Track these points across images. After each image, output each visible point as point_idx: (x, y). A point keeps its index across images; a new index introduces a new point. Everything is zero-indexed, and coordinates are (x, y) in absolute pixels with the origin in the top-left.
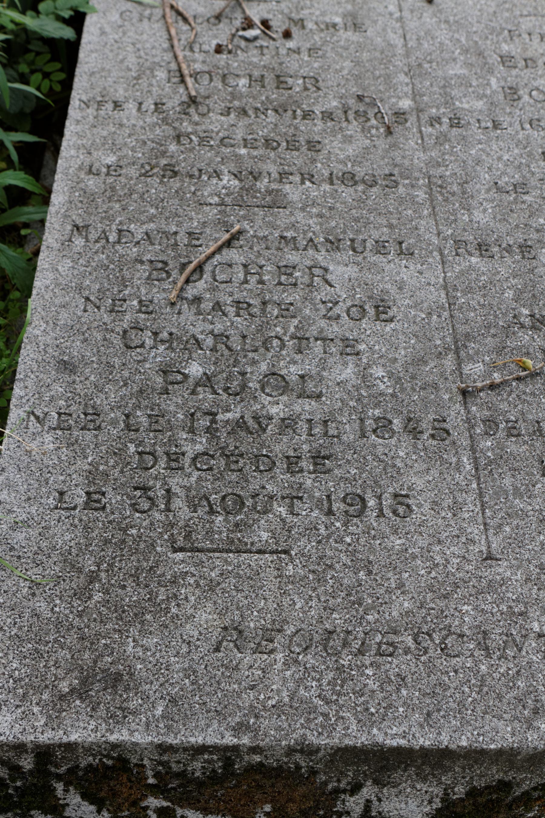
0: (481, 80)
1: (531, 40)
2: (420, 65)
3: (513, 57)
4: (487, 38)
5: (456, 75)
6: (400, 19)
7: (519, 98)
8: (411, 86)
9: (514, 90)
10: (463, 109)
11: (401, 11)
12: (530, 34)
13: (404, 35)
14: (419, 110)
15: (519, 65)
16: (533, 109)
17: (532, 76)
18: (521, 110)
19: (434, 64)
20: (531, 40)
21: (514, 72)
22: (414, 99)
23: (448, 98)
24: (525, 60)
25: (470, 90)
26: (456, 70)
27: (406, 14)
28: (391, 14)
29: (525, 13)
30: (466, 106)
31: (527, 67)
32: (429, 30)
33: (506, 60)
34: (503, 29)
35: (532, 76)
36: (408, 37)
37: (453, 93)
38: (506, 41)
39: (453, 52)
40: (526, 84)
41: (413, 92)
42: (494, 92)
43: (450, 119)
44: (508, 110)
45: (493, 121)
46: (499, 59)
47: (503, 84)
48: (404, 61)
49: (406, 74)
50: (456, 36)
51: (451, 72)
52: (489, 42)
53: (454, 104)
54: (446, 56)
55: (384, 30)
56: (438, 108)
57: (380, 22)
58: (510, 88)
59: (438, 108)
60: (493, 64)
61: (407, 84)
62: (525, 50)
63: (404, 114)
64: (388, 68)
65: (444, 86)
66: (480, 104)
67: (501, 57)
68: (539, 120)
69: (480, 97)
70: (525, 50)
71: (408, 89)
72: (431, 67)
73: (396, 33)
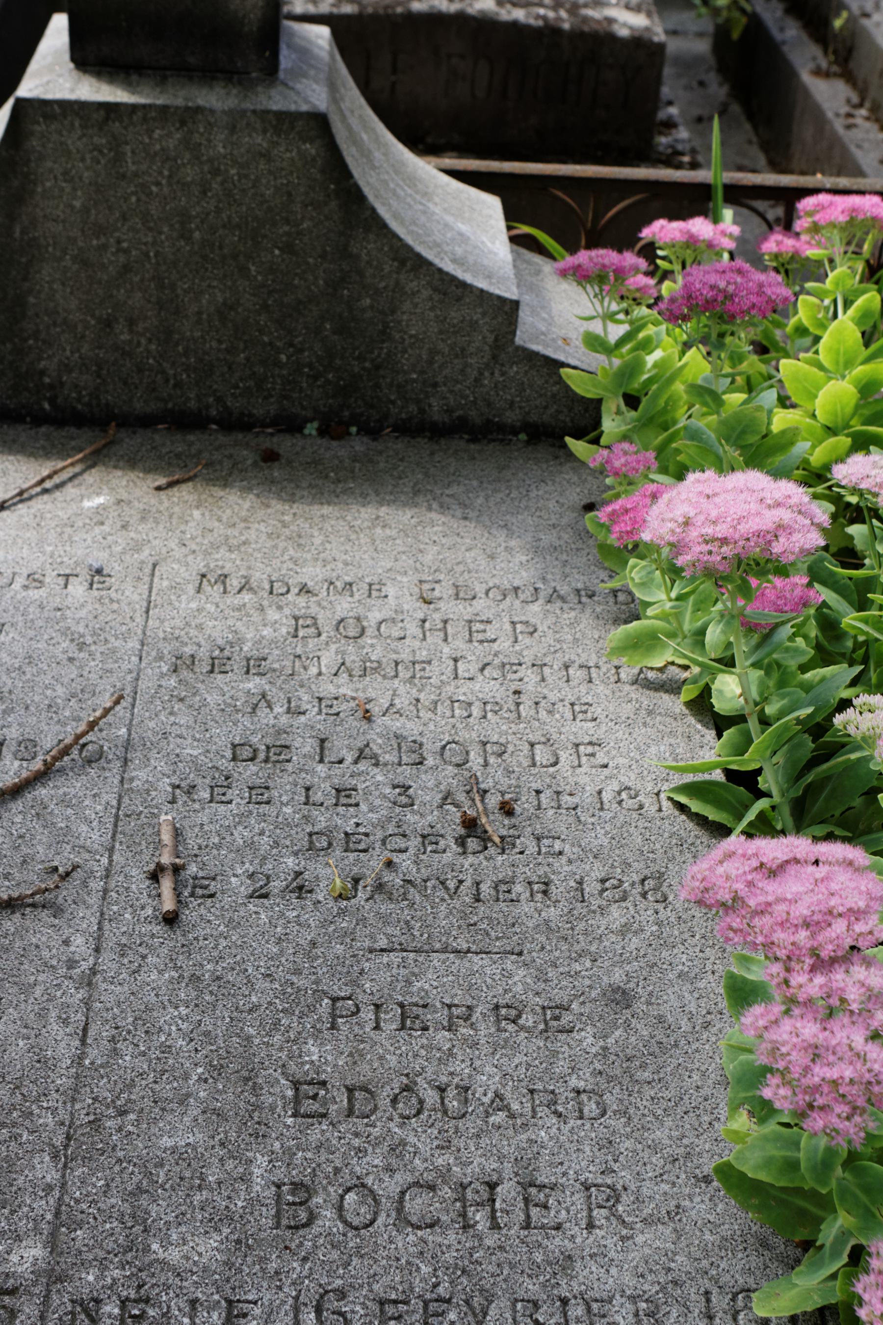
0: (230, 1164)
1: (377, 1027)
2: (96, 1124)
3: (323, 1083)
4: (277, 1024)
5: (174, 1150)
6: (88, 981)
7: (312, 1218)
8: (56, 1193)
9: (303, 1189)
10: (163, 1262)
11: (97, 950)
12: (377, 1007)
13: (85, 1030)
14: (53, 1277)
15: (333, 1108)
16: (335, 1255)
17: (356, 1142)
18: (305, 1259)
19: (132, 1116)
20: (377, 1027)
21: (317, 1132)
22: (52, 1244)
23: (138, 1229)
24: (350, 1090)
25: (197, 1198)
26: (179, 1134)
27: (108, 961)
28: (71, 964)
29: (383, 943)
30: (174, 1255)
31: (350, 1113)
32: (148, 1009)
33: (307, 1093)
34: (319, 994)
35: (356, 1142)
36: (91, 1033)
37: (154, 1209)
38: (317, 1033)
39: (186, 1077)
40: (337, 1170)
41: (57, 1214)
42: (253, 1202)
43: (124, 1303)
44: (273, 1266)
45: (230, 1302)
46: (290, 1093)
47: (280, 1174)
48: (64, 1115)
49: (55, 1157)
50: (208, 1023)
51: (167, 1142)
52: (277, 1038)
53: (147, 1249)
54: (166, 1089)
55: (42, 1014)
56: (103, 1265)
57: (38, 991)
58: (297, 1186)
59: (103, 1265)
60: (272, 1109)
61: (49, 1188)
62: (356, 1056)
63: (12, 1292)
64: (16, 1137)
65: (140, 1190)
66: (209, 1247)
67: (296, 1085)
68: (341, 1294)
69: (214, 1224)
70: (356, 1056)
71: (44, 1207)
72: (120, 1130)
73: (66, 1022)
